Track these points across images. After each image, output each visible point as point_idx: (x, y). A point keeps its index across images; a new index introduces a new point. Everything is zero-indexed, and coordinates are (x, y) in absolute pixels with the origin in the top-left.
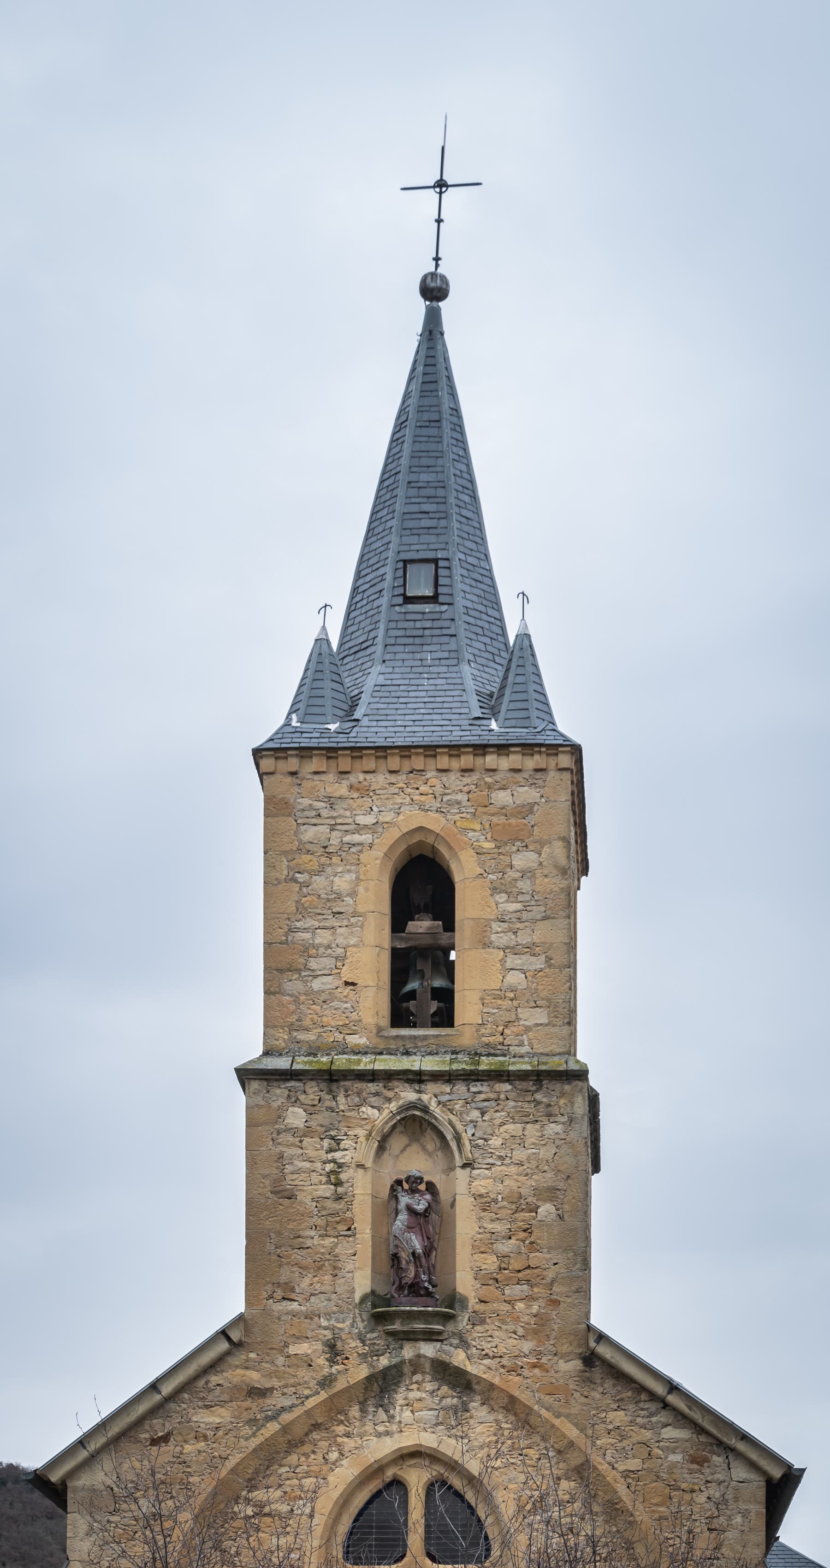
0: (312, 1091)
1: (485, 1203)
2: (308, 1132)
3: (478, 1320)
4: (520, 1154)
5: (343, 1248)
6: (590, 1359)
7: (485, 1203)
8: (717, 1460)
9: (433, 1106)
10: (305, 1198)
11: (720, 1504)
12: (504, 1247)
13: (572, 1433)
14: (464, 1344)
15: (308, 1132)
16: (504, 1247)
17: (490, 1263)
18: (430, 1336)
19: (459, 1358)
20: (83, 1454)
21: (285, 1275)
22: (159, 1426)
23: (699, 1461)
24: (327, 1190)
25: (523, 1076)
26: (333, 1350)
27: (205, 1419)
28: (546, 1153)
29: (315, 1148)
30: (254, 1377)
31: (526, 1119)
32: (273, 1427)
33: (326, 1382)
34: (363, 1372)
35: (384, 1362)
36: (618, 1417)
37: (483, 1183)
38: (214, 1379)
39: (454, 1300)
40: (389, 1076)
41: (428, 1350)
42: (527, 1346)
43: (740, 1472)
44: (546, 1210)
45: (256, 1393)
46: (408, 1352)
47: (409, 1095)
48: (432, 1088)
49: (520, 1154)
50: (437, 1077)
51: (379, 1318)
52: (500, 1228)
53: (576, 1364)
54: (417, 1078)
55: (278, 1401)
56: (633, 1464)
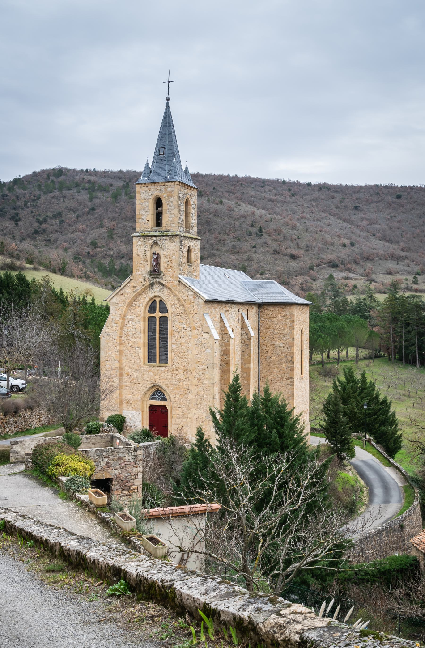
0: (142, 238)
1: (165, 256)
2: (141, 245)
3: (164, 275)
4: (170, 248)
5: (146, 264)
6: (179, 281)
7: (165, 256)
8: (197, 297)
9: (158, 241)
10: (141, 256)
11: (198, 305)
12: (168, 263)
13: (177, 293)
14: (162, 279)
15: (141, 245)
16: (168, 263)
17: (166, 266)
18: (157, 278)
19: (162, 281)
20: (111, 297)
21: (138, 268)
22: (122, 292)
23: (194, 298)
24: (144, 254)
25: (170, 235)
26: (145, 280)
27: (128, 291)
28: (173, 248)
29: (142, 247)
30: (134, 285)
31: (171, 242)
32: (136, 292)
33: (144, 285)
34: (148, 283)
35: (151, 282)
36: (183, 291)
37: (165, 253)
38: (129, 285)
39: (161, 272)
40: (152, 236)
41: (157, 280)
42: (171, 279)
43: (200, 300)
44: (174, 257)
45: (134, 287)
46: (155, 280)
47: (154, 239)
48: (158, 237)
49: (170, 248)
50: (158, 236)
51: (151, 275)
52: (167, 260)
53: (178, 282)
54: (156, 236)
55: (137, 288)
56: (185, 298)
